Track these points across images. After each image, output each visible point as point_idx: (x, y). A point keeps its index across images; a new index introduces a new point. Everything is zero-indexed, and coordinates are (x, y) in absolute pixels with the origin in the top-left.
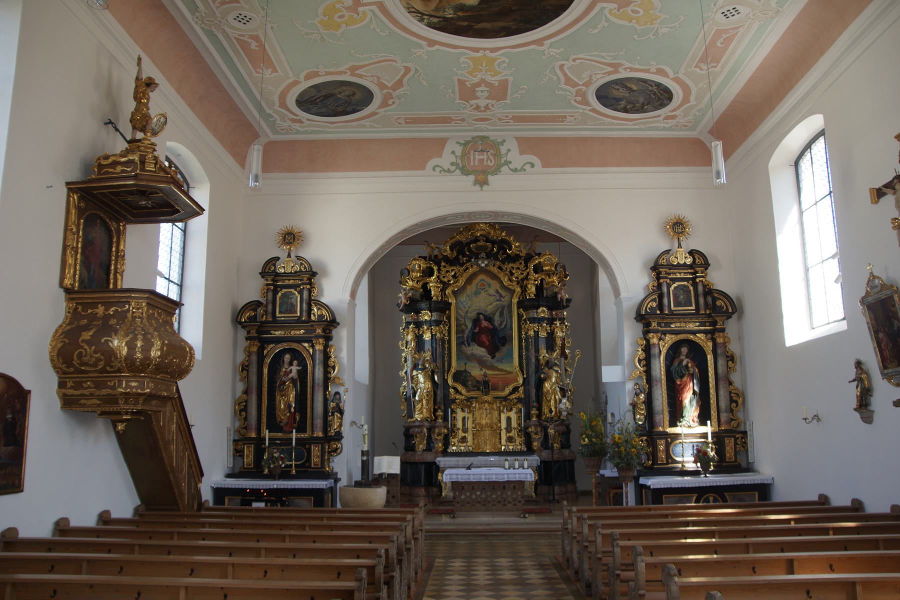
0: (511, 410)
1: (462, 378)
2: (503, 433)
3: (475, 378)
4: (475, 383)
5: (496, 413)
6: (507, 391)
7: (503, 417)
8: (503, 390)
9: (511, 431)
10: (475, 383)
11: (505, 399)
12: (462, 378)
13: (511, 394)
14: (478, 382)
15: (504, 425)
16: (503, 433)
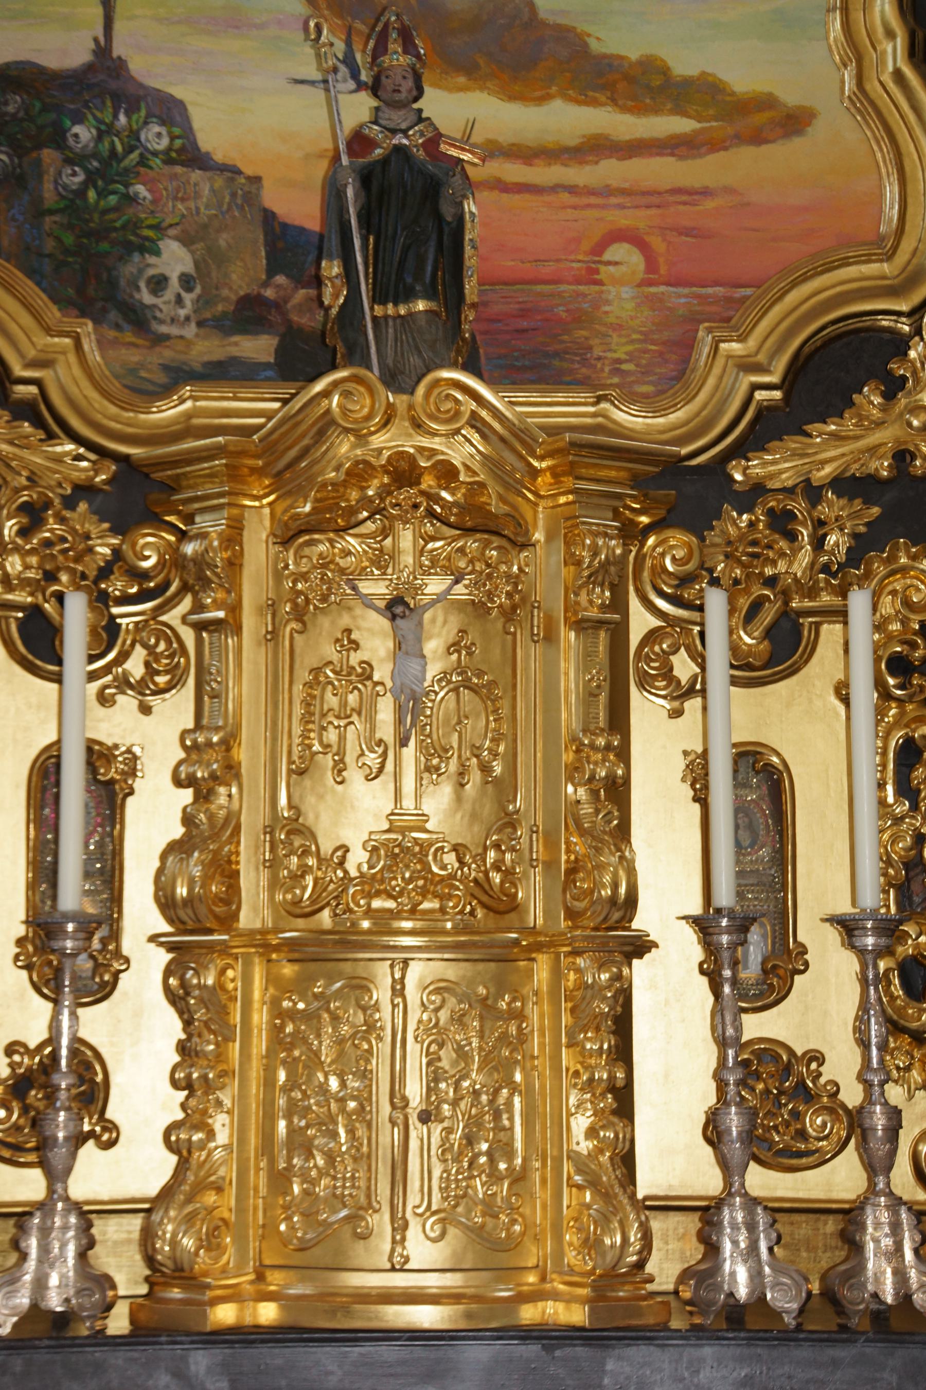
0: (780, 651)
1: (60, 178)
2: (671, 1001)
3: (240, 185)
4: (245, 273)
5: (571, 668)
6: (741, 367)
7: (658, 740)
8: (669, 369)
9: (774, 985)
10: (245, 273)
11: (685, 490)
12: (60, 178)
13: (764, 429)
14: (288, 249)
15: (669, 868)
16: (671, 1001)
